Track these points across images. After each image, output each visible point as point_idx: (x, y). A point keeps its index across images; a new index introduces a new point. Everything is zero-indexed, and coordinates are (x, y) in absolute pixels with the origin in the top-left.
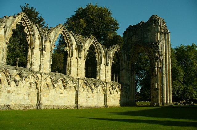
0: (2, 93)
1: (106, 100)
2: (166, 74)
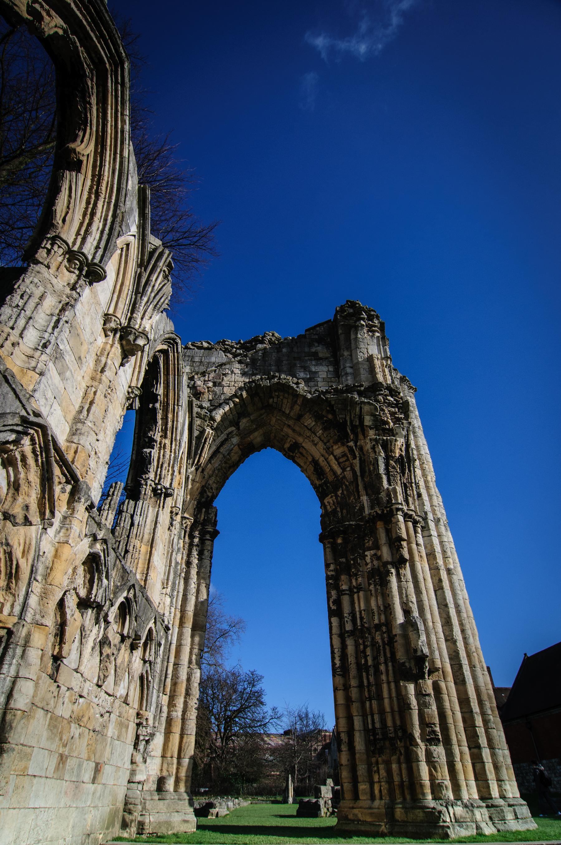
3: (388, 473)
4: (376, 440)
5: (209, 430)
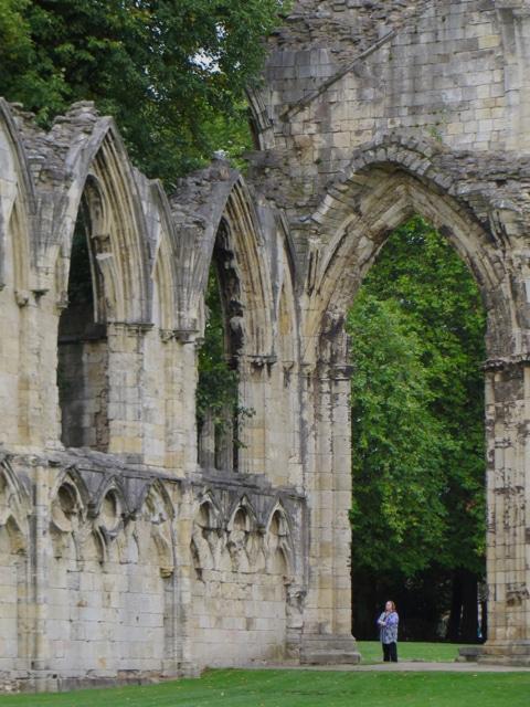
1: (175, 617)
4: (522, 257)
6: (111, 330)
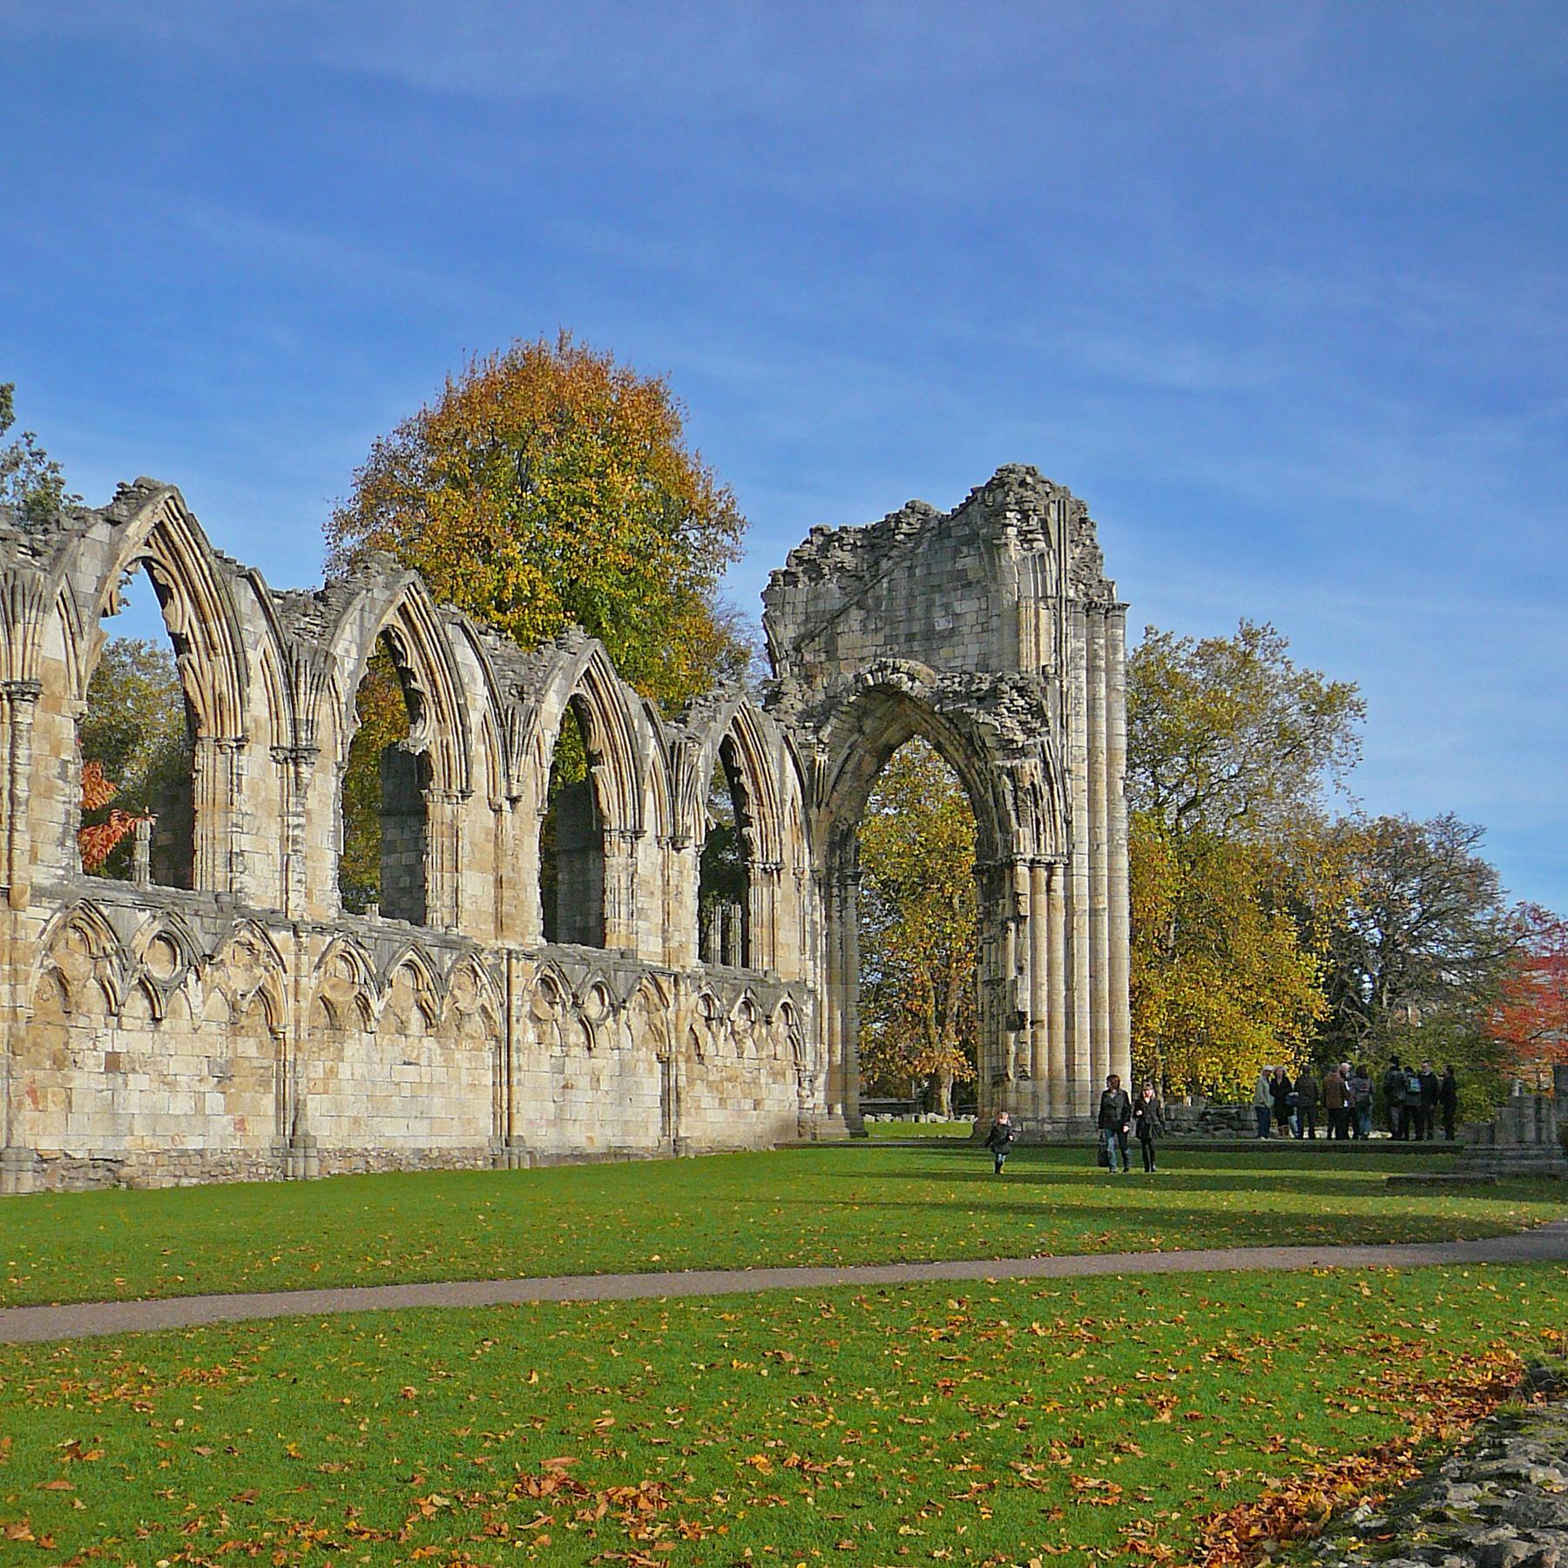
0: (76, 1073)
1: (670, 1099)
2: (1094, 913)
3: (1017, 810)
5: (822, 759)
6: (607, 837)
